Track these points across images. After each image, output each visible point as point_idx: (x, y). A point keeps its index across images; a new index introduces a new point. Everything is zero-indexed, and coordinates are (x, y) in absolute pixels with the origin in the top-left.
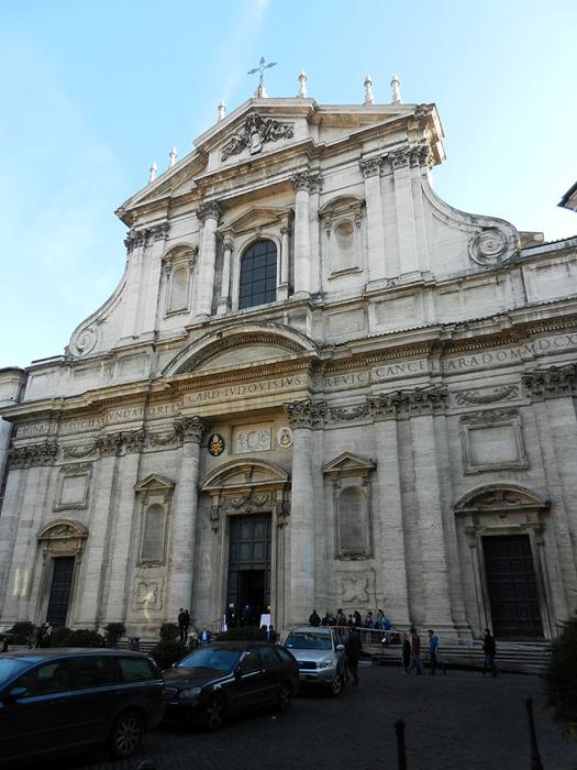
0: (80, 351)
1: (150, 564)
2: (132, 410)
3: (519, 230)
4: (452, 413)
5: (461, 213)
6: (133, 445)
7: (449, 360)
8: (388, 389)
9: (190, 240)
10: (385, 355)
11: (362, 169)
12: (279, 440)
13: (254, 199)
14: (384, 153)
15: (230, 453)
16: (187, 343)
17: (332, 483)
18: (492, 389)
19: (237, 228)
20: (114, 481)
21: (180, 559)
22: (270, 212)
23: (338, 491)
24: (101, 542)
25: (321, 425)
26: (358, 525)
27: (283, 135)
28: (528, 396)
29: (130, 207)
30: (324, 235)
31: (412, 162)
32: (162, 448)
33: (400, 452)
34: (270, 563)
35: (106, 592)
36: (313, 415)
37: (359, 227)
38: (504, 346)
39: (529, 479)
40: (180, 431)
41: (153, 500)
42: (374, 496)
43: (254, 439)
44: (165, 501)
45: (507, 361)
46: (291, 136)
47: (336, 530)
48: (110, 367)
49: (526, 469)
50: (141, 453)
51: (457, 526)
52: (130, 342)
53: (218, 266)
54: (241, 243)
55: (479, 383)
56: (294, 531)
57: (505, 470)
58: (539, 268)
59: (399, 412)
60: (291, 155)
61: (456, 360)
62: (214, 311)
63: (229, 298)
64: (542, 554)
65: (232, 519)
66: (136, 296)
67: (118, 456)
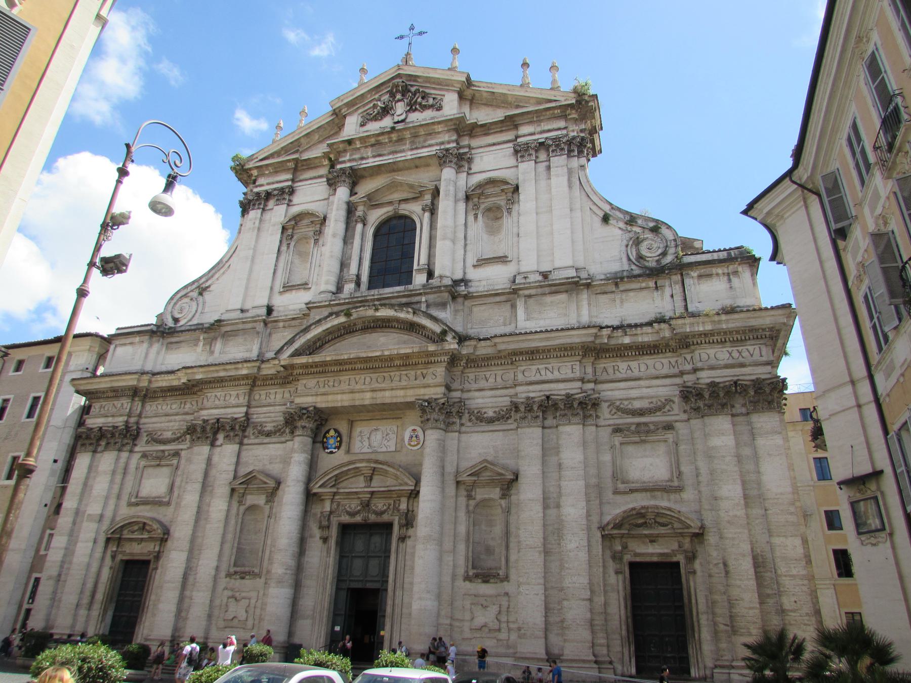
0: (176, 320)
1: (243, 575)
2: (234, 393)
3: (680, 235)
4: (603, 424)
6: (232, 434)
7: (603, 366)
8: (536, 392)
9: (318, 208)
10: (532, 354)
11: (516, 152)
13: (394, 171)
14: (541, 137)
15: (348, 451)
16: (305, 323)
17: (465, 493)
18: (647, 401)
19: (372, 201)
20: (206, 474)
22: (411, 186)
23: (472, 503)
24: (186, 545)
25: (456, 427)
26: (491, 543)
27: (431, 106)
28: (685, 411)
30: (471, 218)
31: (570, 151)
32: (267, 440)
33: (544, 463)
34: (387, 581)
35: (185, 605)
36: (449, 414)
38: (661, 356)
39: (682, 501)
40: (291, 422)
42: (513, 511)
43: (377, 438)
44: (267, 502)
45: (665, 371)
46: (440, 108)
47: (467, 547)
48: (210, 342)
49: (679, 489)
50: (241, 444)
51: (603, 551)
52: (238, 314)
53: (347, 240)
54: (376, 216)
55: (634, 393)
56: (420, 547)
57: (658, 490)
58: (700, 277)
59: (544, 419)
60: (439, 128)
62: (339, 289)
63: (358, 277)
64: (692, 584)
65: (345, 529)
66: (249, 263)
67: (213, 445)
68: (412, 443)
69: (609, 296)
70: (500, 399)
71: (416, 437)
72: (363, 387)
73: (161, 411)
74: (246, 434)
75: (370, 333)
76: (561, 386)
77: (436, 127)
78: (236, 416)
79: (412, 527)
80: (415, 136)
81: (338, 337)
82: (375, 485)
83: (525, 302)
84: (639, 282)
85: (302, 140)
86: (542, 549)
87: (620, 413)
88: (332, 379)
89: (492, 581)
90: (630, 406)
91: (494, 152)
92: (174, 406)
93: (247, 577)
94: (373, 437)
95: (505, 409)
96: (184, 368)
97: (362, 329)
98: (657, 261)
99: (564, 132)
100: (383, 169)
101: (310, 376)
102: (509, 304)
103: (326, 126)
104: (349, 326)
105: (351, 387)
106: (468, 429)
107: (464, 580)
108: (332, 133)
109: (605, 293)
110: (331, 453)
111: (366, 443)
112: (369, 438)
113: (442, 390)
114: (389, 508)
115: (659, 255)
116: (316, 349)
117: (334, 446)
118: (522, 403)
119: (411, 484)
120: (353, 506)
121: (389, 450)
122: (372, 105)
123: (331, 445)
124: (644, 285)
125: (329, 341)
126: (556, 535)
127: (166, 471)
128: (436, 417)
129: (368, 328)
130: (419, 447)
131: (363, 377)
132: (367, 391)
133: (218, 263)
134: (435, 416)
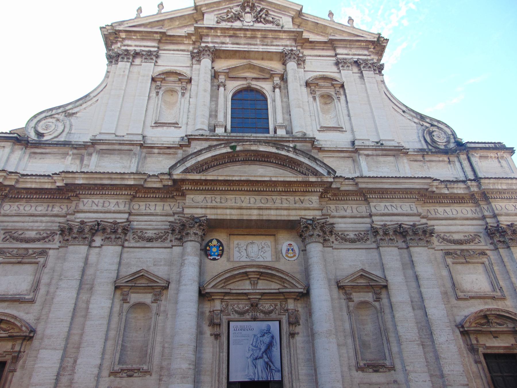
0: (40, 135)
1: (130, 373)
2: (113, 201)
5: (414, 111)
6: (113, 236)
8: (391, 221)
11: (337, 64)
12: (284, 252)
14: (355, 58)
15: (228, 260)
18: (463, 234)
19: (230, 73)
21: (185, 366)
23: (351, 304)
26: (366, 338)
27: (272, 22)
28: (491, 244)
29: (121, 28)
32: (149, 244)
36: (324, 233)
37: (339, 100)
41: (135, 298)
44: (155, 301)
45: (470, 215)
50: (123, 246)
52: (112, 137)
53: (214, 97)
54: (233, 86)
55: (453, 229)
58: (481, 157)
60: (284, 36)
61: (431, 209)
68: (289, 255)
69: (419, 163)
70: (358, 225)
71: (292, 250)
73: (23, 212)
74: (127, 238)
75: (250, 165)
76: (405, 218)
77: (281, 34)
78: (119, 221)
79: (299, 325)
80: (265, 37)
81: (222, 164)
82: (261, 288)
83: (366, 159)
84: (438, 157)
85: (166, 22)
86: (419, 342)
87: (445, 242)
88: (218, 197)
89: (381, 370)
90: (451, 238)
91: (320, 61)
92: (39, 208)
93: (136, 375)
94: (249, 249)
95: (363, 233)
96: (63, 172)
97: (244, 160)
98: (445, 146)
99: (369, 58)
100: (238, 54)
101: (198, 192)
102: (350, 159)
103: (186, 17)
104: (233, 156)
105: (238, 205)
107: (357, 371)
108: (189, 23)
109: (416, 161)
110: (214, 259)
111: (244, 254)
112: (246, 250)
114: (275, 308)
115: (445, 142)
116: (203, 171)
117: (216, 254)
118: (380, 228)
119: (300, 287)
121: (266, 260)
122: (225, 11)
123: (214, 253)
124: (441, 159)
125: (214, 166)
126: (424, 331)
127: (29, 268)
128: (317, 233)
129: (249, 160)
130: (295, 258)
131: (248, 197)
132: (254, 209)
133: (86, 96)
134: (316, 232)
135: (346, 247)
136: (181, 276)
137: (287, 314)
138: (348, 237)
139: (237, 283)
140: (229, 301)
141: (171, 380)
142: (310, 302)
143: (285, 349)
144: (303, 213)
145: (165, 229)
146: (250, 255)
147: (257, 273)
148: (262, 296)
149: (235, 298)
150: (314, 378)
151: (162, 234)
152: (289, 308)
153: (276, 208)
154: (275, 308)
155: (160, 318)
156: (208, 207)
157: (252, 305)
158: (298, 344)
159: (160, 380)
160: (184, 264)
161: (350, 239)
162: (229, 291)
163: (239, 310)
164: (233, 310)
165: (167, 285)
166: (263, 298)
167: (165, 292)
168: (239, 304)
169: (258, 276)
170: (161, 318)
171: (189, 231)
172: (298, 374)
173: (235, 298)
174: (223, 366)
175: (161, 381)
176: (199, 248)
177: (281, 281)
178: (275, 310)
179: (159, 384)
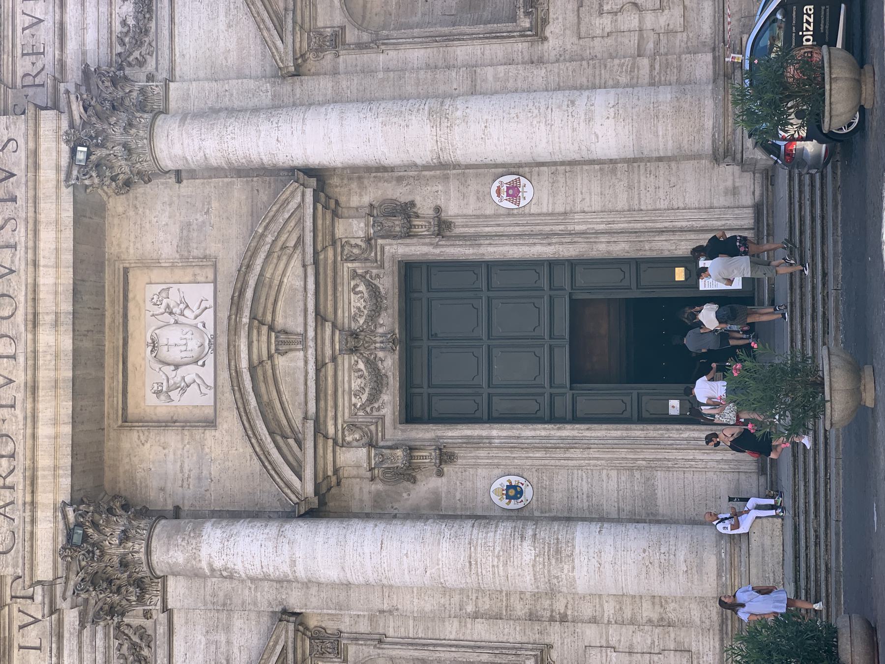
17: (329, 56)
21: (527, 552)
23: (351, 36)
25: (156, 88)
47: (460, 38)
72: (21, 359)
79: (412, 204)
82: (301, 320)
94: (175, 355)
105: (20, 396)
106: (164, 63)
107: (544, 39)
111: (190, 373)
112: (177, 366)
113: (48, 119)
114: (362, 277)
119: (298, 199)
120: (356, 384)
121: (211, 302)
128: (118, 130)
132: (35, 341)
134: (117, 134)
135: (166, 32)
136: (266, 578)
137: (380, 241)
138: (131, 22)
139: (286, 397)
140: (340, 421)
141: (564, 590)
142: (343, 168)
143: (482, 250)
144: (48, 175)
145: (106, 636)
146: (195, 354)
147: (255, 332)
148: (325, 320)
149: (330, 403)
150: (561, 169)
151: (125, 647)
152: (361, 234)
153: (31, 269)
154: (362, 277)
155: (391, 632)
156: (28, 499)
157: (353, 350)
158: (470, 212)
159: (563, 619)
160: (226, 569)
161: (140, 16)
162: (310, 424)
163: (367, 390)
164: (368, 409)
165: (292, 619)
166: (330, 316)
167: (312, 623)
168: (350, 388)
169: (265, 329)
170: (392, 628)
171: (116, 560)
172: (552, 214)
173: (330, 403)
174: (527, 438)
175: (566, 615)
176: (175, 521)
177: (279, 258)
178: (368, 277)
179: (573, 622)
